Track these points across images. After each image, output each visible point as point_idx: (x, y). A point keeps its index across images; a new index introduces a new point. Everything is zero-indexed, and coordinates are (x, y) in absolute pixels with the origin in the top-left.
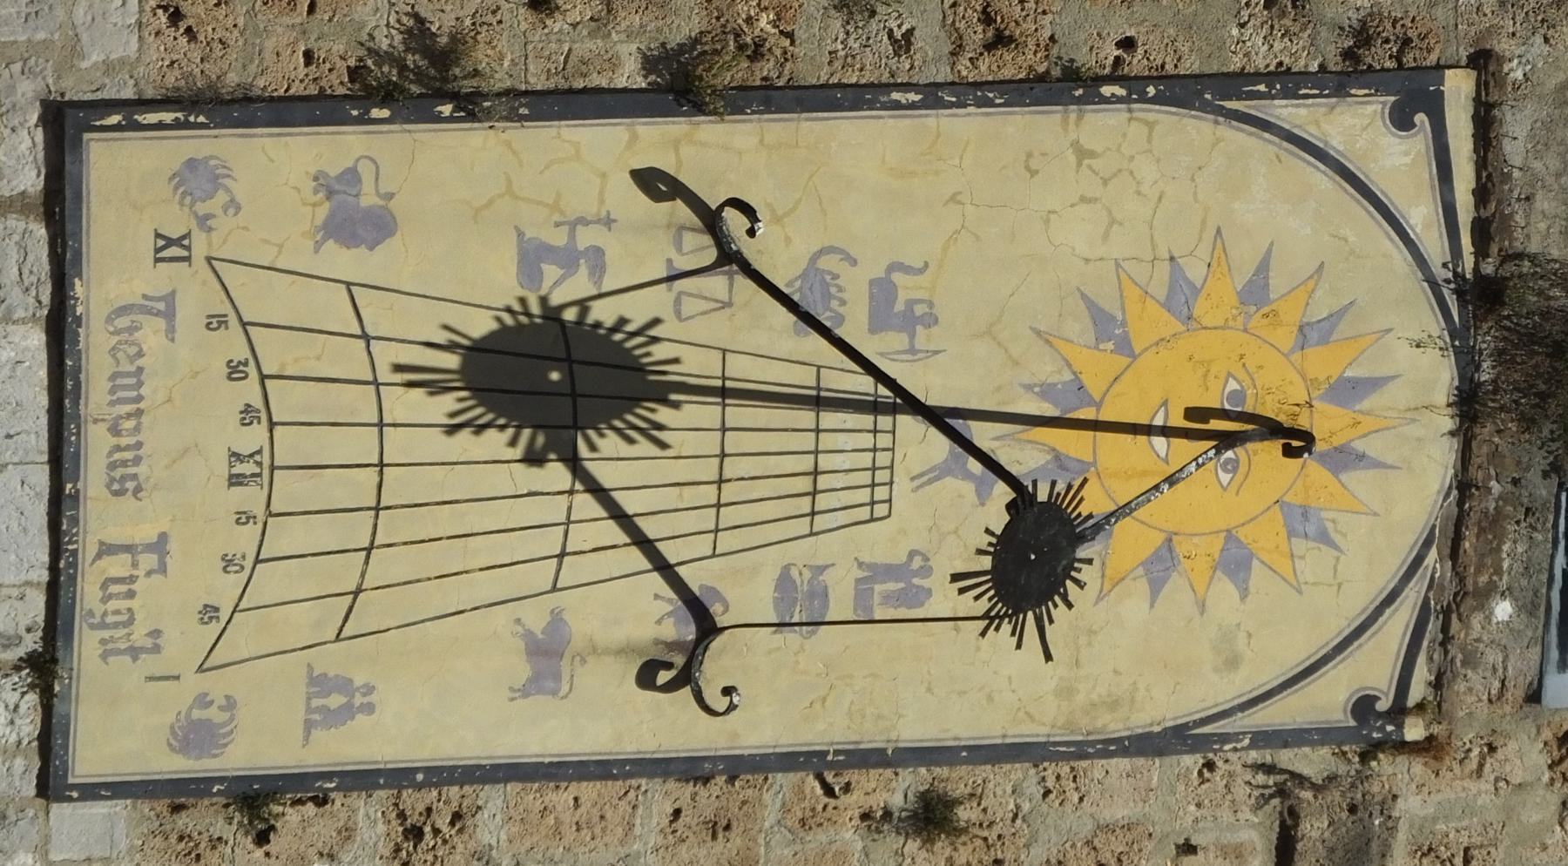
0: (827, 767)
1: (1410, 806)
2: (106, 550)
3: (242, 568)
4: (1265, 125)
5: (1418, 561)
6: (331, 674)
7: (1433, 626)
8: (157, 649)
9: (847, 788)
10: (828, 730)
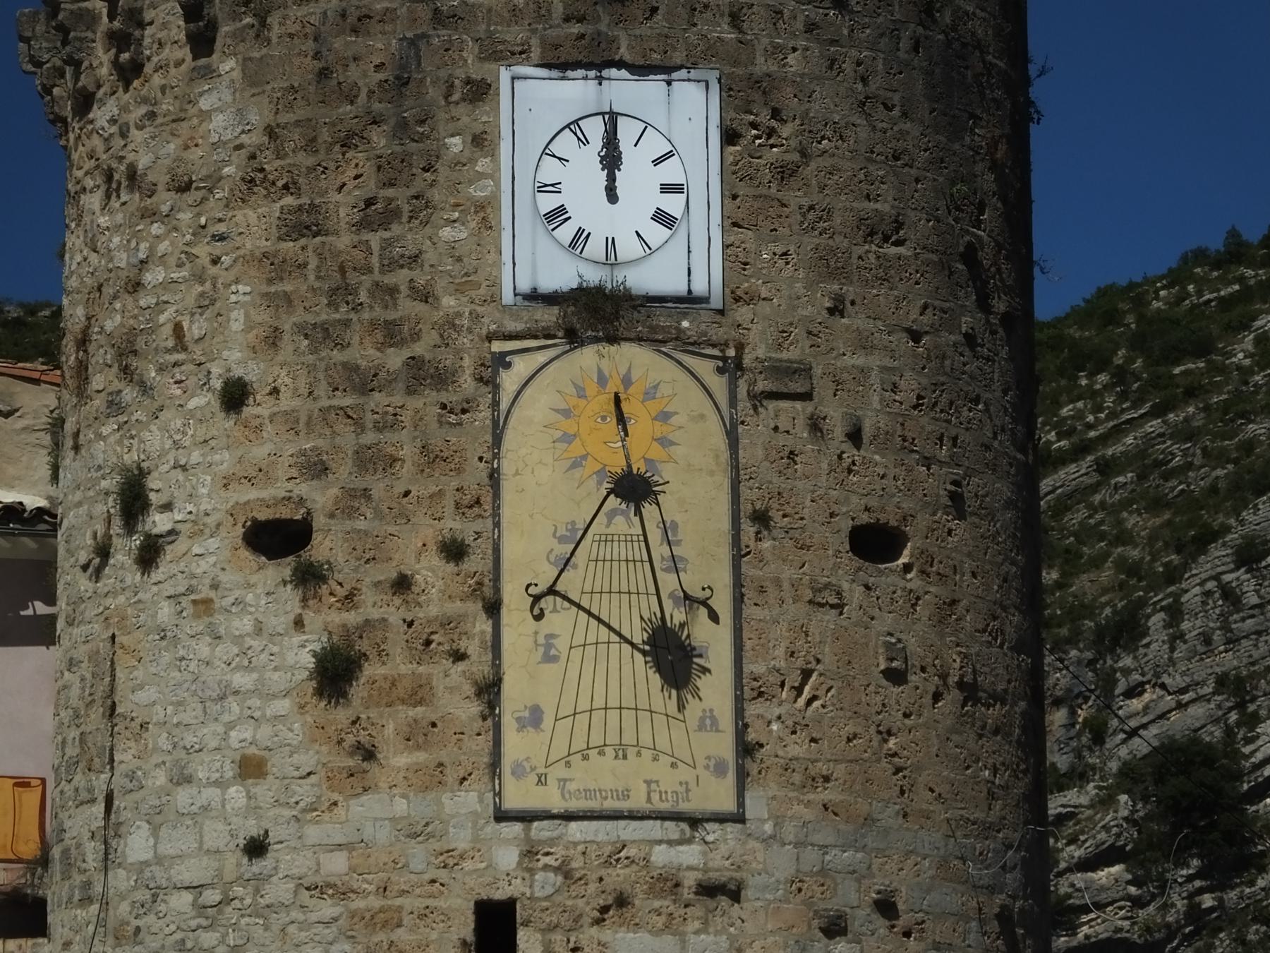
0: (739, 554)
1: (761, 352)
2: (649, 800)
4: (509, 412)
5: (665, 354)
7: (690, 348)
8: (687, 783)
9: (747, 546)
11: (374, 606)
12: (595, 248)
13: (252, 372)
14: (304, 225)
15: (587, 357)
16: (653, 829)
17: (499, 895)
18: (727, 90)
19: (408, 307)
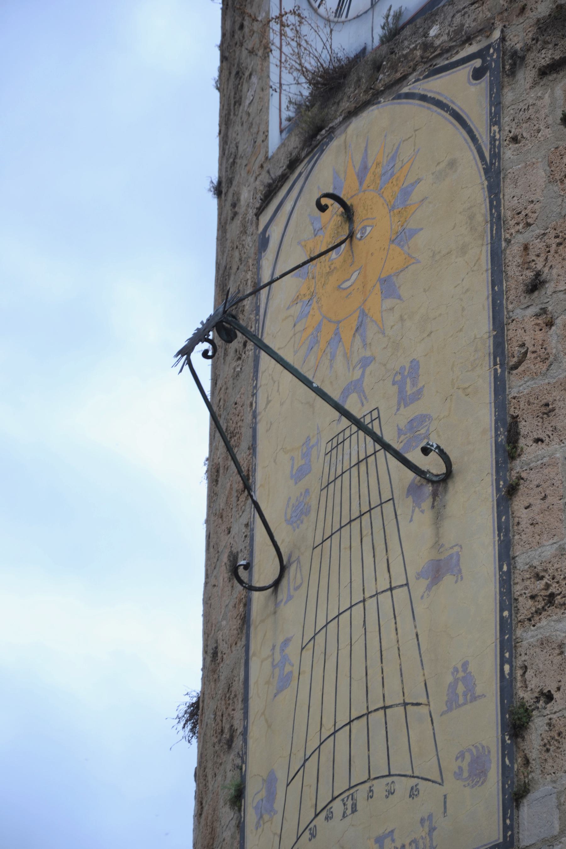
3: (393, 782)
6: (446, 698)
7: (442, 62)
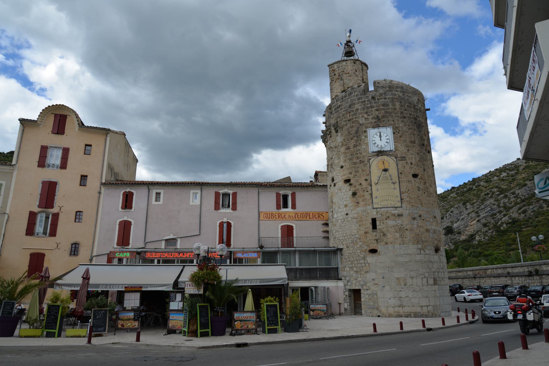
10: (397, 178)
11: (358, 187)
12: (380, 146)
13: (343, 164)
14: (348, 148)
15: (380, 158)
16: (391, 209)
17: (374, 217)
18: (393, 128)
19: (359, 155)
